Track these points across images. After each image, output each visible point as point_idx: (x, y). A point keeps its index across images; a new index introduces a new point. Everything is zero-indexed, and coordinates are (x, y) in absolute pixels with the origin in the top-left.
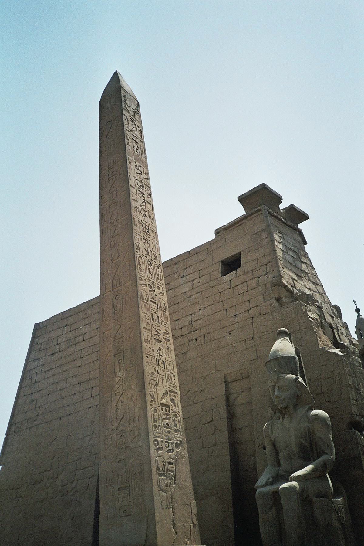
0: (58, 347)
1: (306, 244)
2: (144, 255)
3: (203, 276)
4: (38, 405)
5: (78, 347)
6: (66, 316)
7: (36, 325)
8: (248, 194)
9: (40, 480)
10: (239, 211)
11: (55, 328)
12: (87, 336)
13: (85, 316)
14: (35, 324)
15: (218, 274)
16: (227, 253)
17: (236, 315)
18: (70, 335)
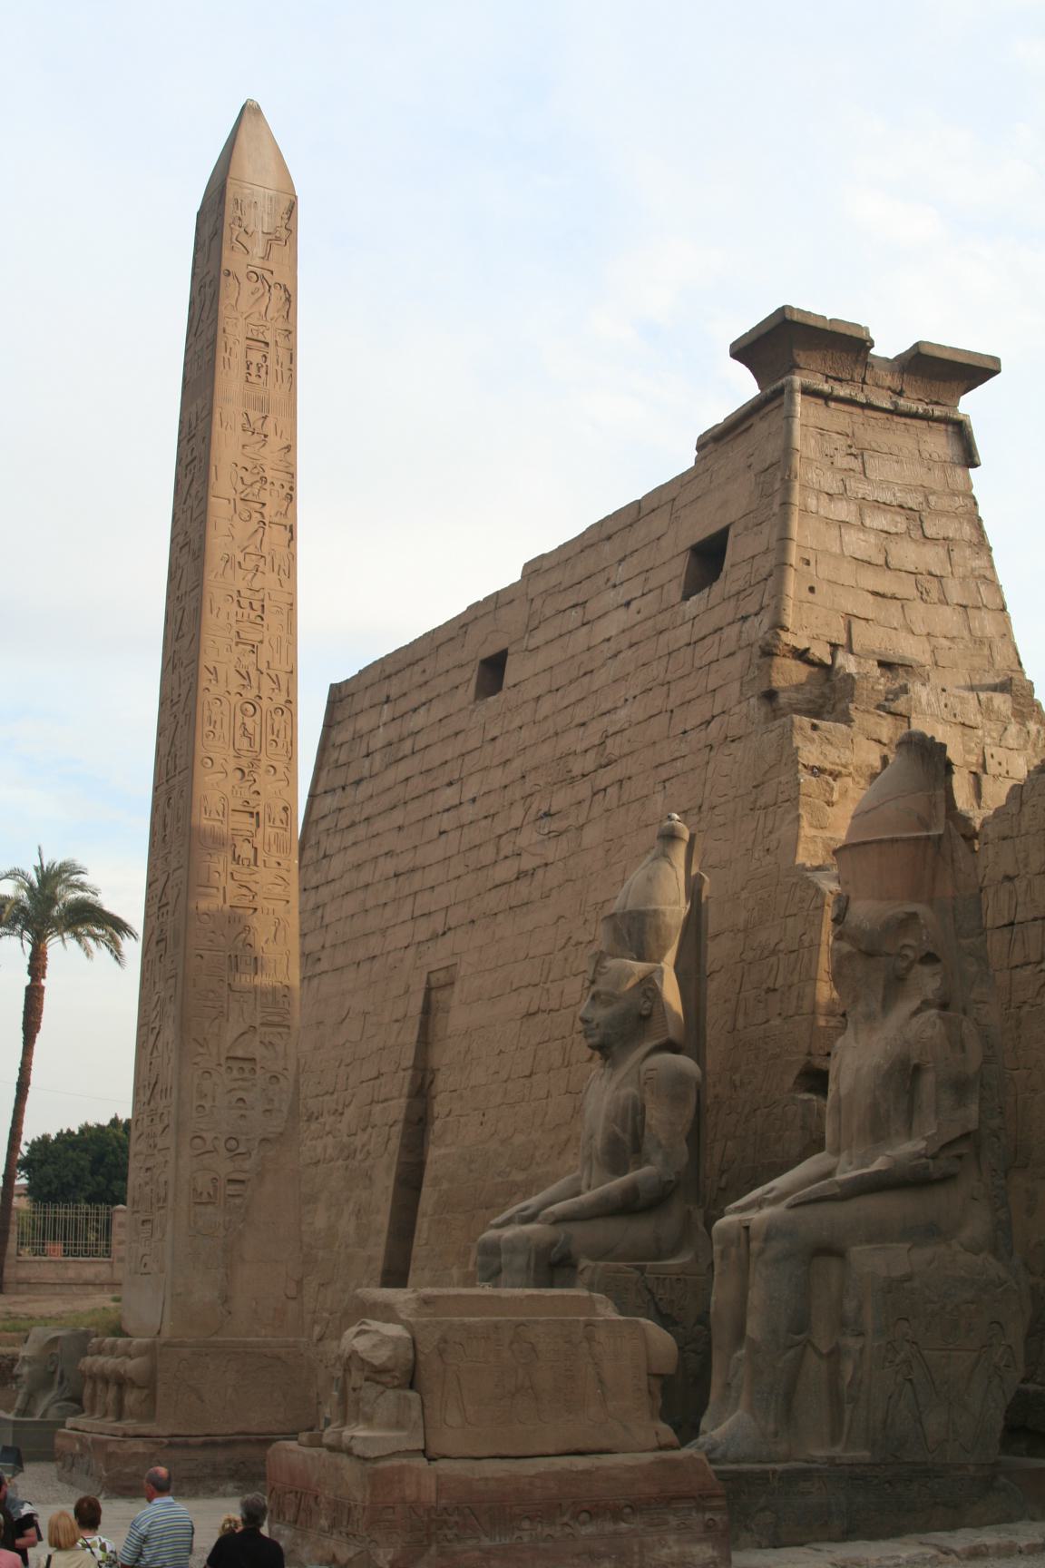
0: (367, 762)
1: (975, 465)
2: (234, 691)
3: (650, 591)
4: (327, 920)
5: (402, 770)
6: (389, 670)
7: (335, 689)
8: (754, 337)
9: (316, 1114)
10: (743, 386)
11: (366, 704)
12: (422, 741)
13: (423, 679)
14: (332, 685)
15: (675, 591)
16: (699, 528)
17: (685, 732)
18: (392, 732)
